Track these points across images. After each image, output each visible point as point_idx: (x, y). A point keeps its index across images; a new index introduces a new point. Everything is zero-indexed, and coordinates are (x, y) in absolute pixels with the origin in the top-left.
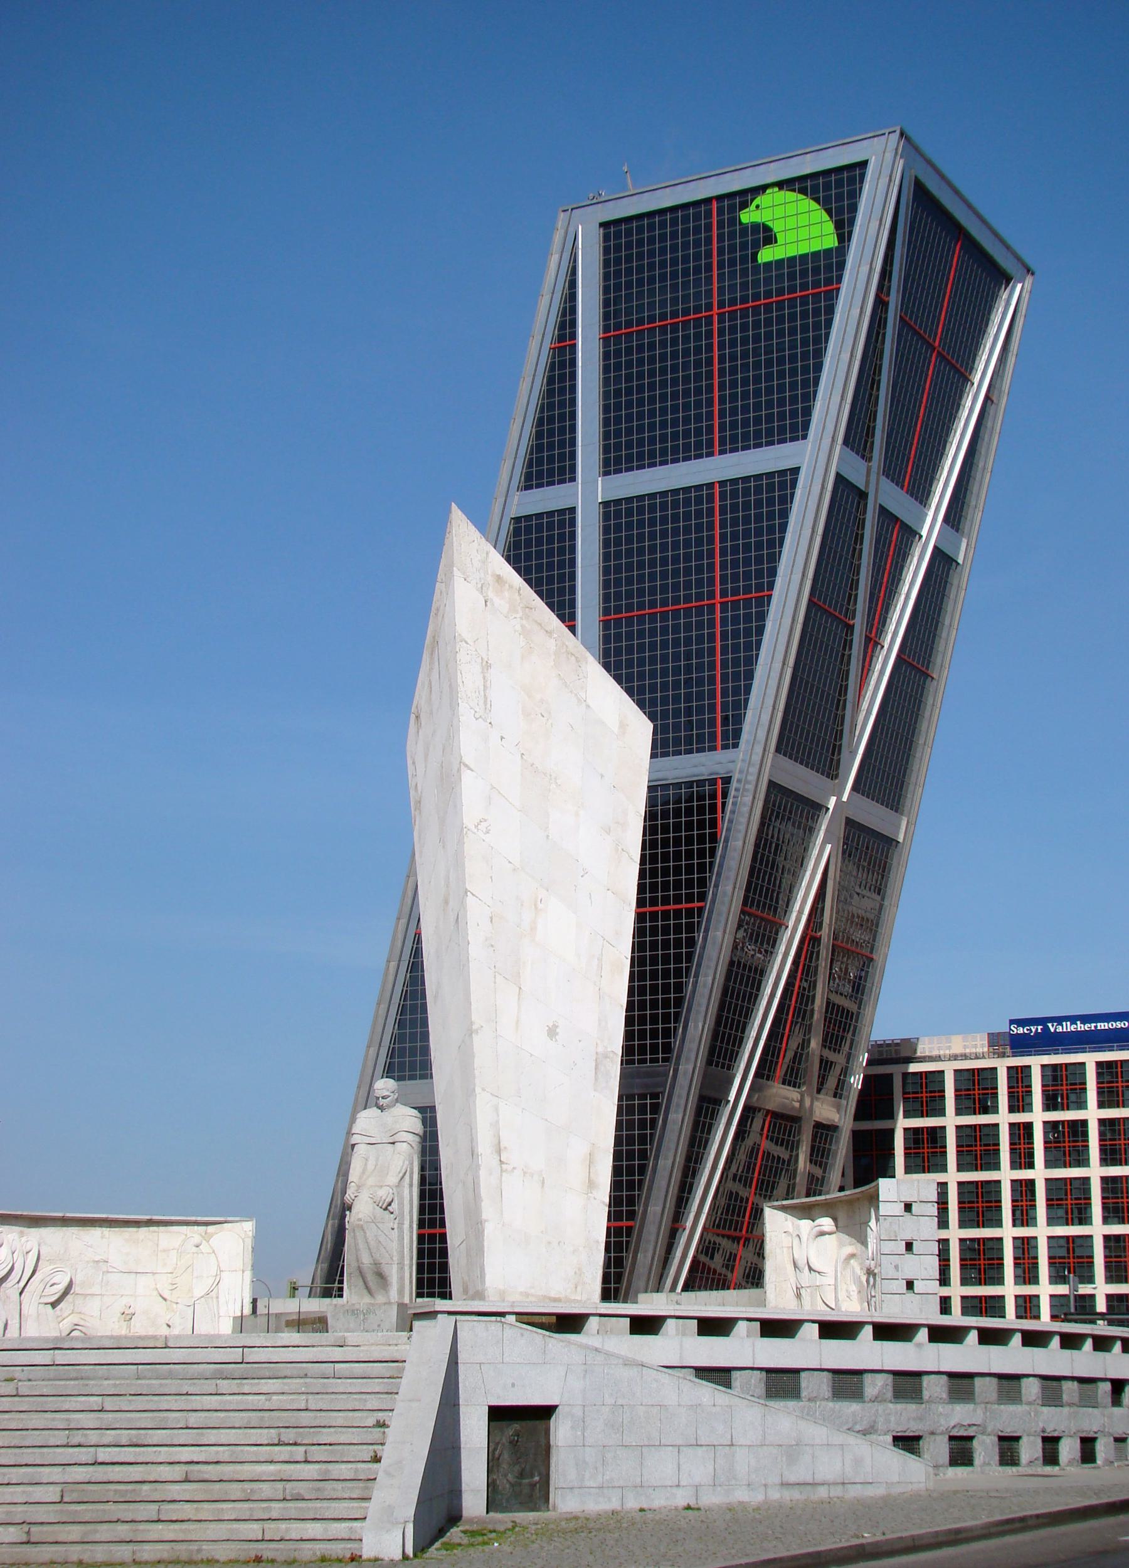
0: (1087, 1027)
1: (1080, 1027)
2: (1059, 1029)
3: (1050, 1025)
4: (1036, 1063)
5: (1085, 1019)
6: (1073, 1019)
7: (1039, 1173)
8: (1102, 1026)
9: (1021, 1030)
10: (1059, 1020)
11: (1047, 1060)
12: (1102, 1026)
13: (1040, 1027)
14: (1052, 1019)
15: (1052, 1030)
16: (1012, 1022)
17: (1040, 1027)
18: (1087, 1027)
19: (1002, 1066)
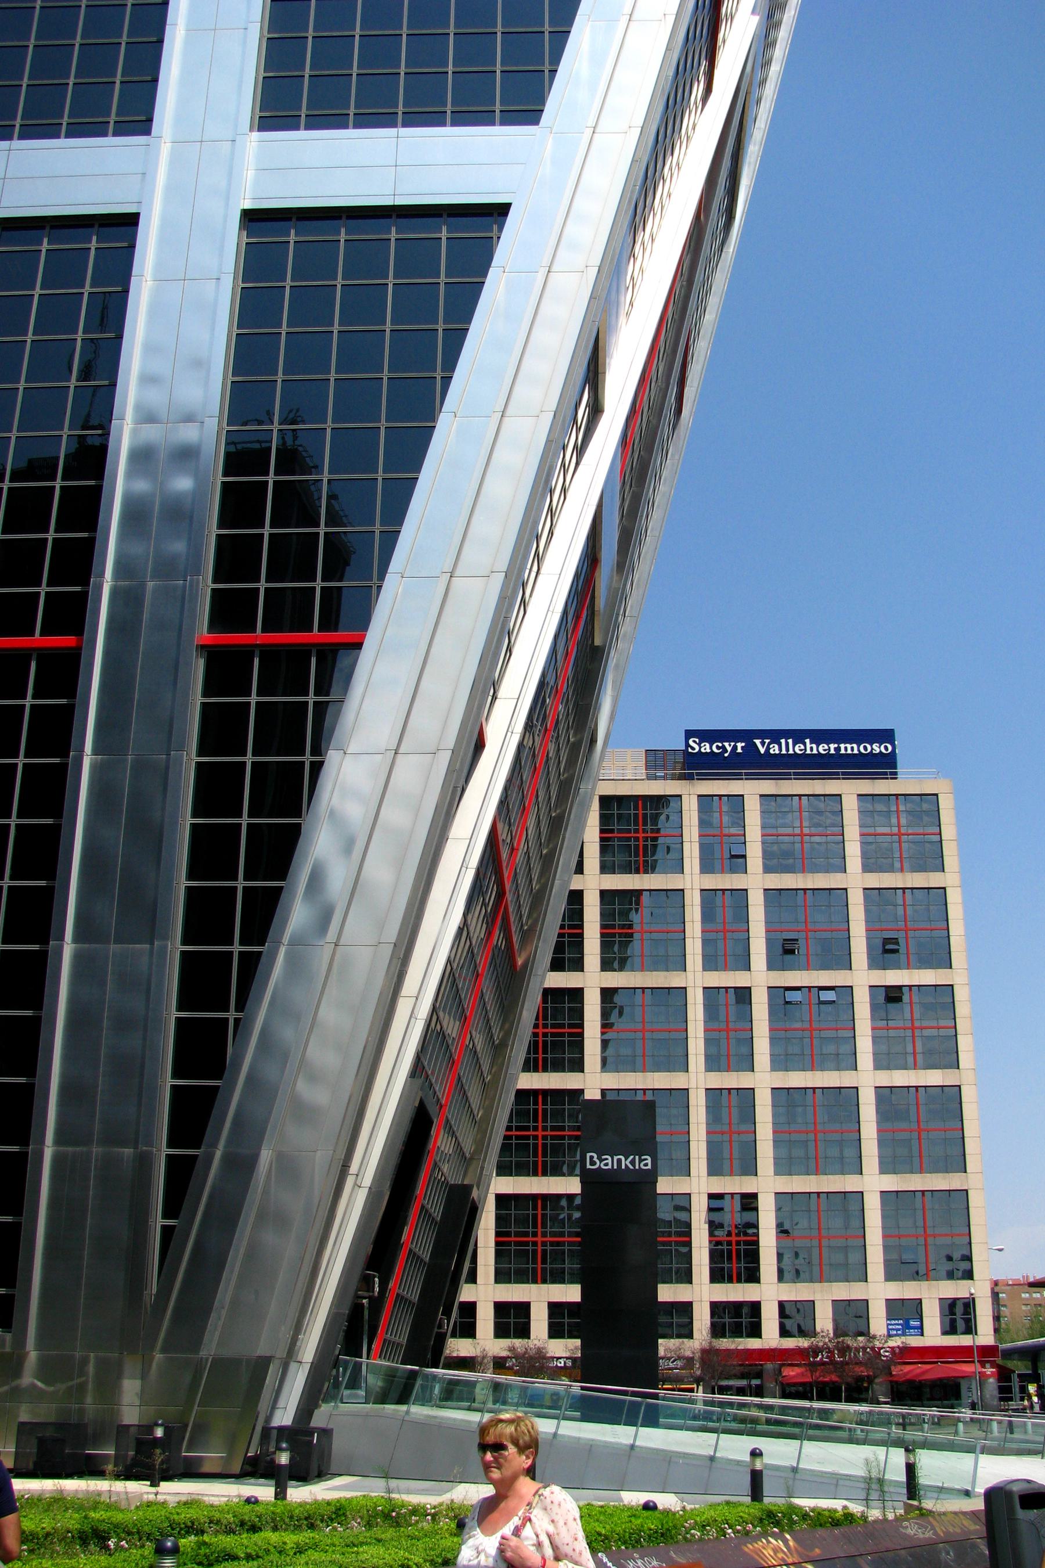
0: (822, 749)
1: (810, 747)
2: (775, 749)
3: (758, 742)
4: (752, 790)
5: (819, 736)
6: (799, 736)
7: (760, 977)
8: (848, 748)
9: (706, 748)
10: (776, 735)
11: (768, 787)
12: (848, 748)
13: (740, 745)
14: (762, 734)
15: (762, 750)
16: (689, 734)
17: (740, 745)
18: (822, 749)
19: (690, 795)
